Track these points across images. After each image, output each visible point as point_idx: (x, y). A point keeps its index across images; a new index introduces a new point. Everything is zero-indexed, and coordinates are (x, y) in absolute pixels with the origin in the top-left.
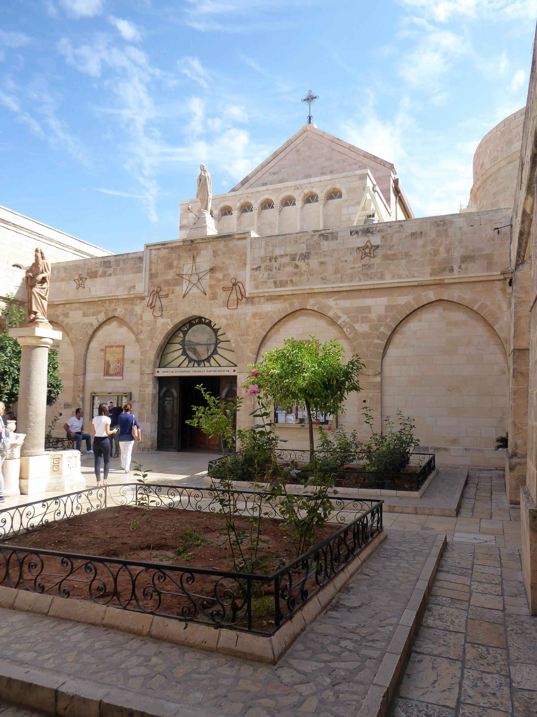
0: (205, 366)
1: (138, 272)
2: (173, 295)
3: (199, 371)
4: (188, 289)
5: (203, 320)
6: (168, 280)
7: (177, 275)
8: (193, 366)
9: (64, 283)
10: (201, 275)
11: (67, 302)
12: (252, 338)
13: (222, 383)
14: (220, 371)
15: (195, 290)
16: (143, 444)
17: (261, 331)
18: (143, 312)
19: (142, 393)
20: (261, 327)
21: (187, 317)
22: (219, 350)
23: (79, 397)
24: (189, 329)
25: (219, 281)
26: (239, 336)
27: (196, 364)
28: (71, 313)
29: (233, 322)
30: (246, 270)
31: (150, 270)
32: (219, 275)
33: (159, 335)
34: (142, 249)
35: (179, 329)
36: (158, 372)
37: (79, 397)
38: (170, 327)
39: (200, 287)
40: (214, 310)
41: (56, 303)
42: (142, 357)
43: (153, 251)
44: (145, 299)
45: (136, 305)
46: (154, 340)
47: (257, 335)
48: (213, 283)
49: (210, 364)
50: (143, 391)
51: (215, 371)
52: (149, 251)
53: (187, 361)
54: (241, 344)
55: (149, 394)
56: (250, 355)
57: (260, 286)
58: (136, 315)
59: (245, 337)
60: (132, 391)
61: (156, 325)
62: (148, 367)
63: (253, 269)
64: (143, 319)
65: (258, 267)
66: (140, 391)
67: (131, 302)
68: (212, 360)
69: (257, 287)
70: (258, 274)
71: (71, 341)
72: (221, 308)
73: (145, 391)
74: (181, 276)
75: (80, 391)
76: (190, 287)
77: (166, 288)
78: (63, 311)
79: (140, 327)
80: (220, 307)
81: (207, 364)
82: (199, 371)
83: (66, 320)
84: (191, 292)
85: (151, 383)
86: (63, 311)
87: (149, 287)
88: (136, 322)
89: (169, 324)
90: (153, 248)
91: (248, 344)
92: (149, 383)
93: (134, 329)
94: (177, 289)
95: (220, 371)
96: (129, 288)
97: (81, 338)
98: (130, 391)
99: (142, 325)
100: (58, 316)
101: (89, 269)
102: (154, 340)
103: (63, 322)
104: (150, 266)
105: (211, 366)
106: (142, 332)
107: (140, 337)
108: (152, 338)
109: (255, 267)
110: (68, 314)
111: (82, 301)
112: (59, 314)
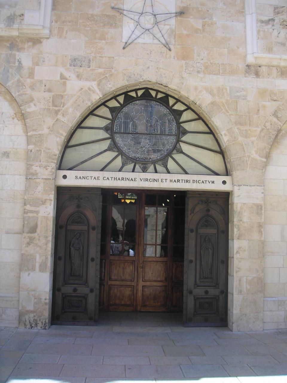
0: (156, 172)
2: (104, 42)
3: (154, 180)
4: (134, 37)
5: (153, 93)
6: (93, 15)
7: (113, 8)
8: (133, 171)
10: (159, 18)
12: (259, 129)
13: (190, 204)
14: (198, 182)
15: (147, 39)
16: (32, 315)
17: (275, 120)
18: (37, 65)
19: (30, 215)
20: (275, 114)
21: (133, 82)
22: (185, 147)
24: (123, 106)
25: (197, 31)
26: (236, 123)
27: (137, 166)
29: (224, 101)
30: (245, 22)
32: (195, 22)
33: (71, 110)
35: (104, 104)
36: (65, 177)
38: (97, 97)
39: (159, 35)
40: (185, 75)
44: (41, 42)
45: (19, 50)
47: (268, 125)
48: (185, 32)
49: (167, 169)
50: (31, 212)
51: (187, 181)
53: (119, 161)
54: (240, 139)
55: (47, 218)
56: (257, 157)
57: (275, 49)
58: (20, 67)
59: (247, 128)
61: (64, 91)
62: (46, 167)
63: (262, 22)
64: (37, 77)
65: (270, 20)
66: (25, 212)
68: (171, 164)
69: (269, 50)
70: (271, 30)
72: (199, 75)
73: (37, 212)
74: (120, 11)
76: (137, 33)
77: (89, 29)
79: (29, 91)
80: (198, 72)
81: (159, 168)
82: (154, 180)
84: (140, 40)
88: (19, 81)
89: (94, 92)
91: (254, 139)
92: (45, 197)
93: (15, 94)
94: (112, 31)
95: (198, 182)
99: (32, 88)
102: (60, 116)
105: (169, 172)
106: (32, 100)
107: (29, 110)
108: (57, 112)
109: (265, 18)
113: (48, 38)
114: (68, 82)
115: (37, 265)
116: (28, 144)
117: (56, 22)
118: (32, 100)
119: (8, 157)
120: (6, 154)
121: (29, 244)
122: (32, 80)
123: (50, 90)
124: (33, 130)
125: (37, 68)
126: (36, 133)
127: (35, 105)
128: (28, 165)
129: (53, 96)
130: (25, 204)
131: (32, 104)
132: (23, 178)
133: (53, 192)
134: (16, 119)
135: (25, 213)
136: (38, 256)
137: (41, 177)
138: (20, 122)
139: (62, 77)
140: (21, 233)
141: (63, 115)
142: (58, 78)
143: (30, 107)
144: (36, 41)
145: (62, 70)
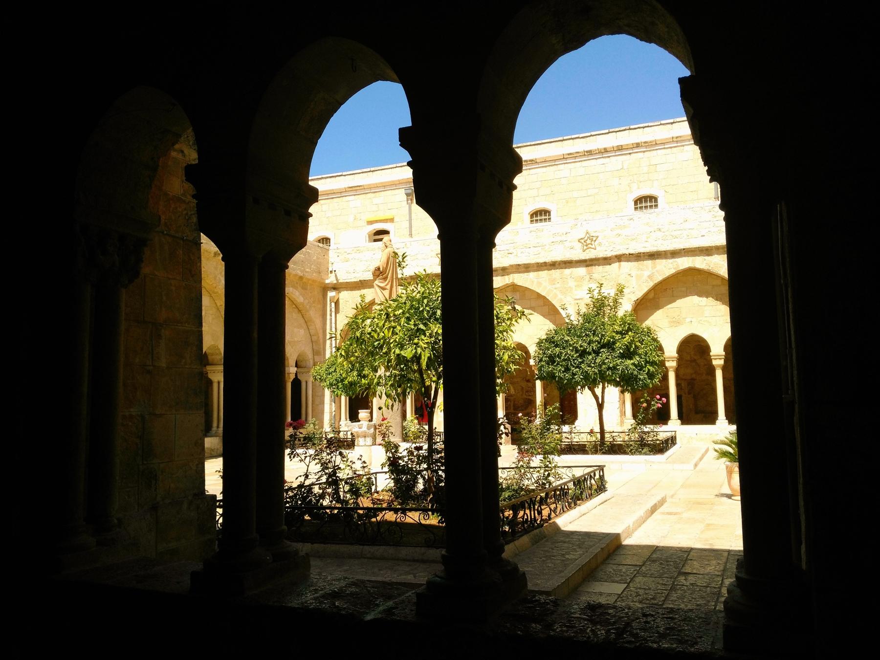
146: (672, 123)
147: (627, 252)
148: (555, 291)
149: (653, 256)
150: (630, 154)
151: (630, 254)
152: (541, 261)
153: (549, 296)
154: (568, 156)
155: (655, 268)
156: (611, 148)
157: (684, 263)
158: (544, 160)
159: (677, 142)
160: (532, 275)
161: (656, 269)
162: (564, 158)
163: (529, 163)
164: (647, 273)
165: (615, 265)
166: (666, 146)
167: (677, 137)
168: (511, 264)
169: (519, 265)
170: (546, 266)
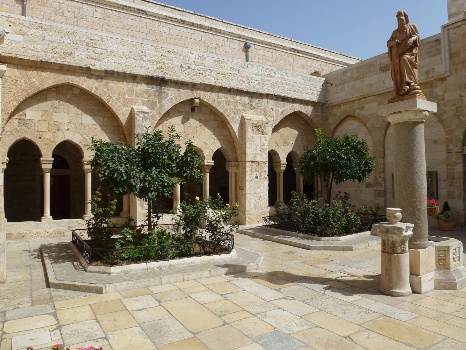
1: (435, 55)
9: (357, 82)
11: (362, 97)
18: (445, 92)
23: (380, 177)
28: (367, 106)
31: (450, 50)
34: (438, 31)
37: (380, 177)
41: (351, 100)
42: (447, 136)
43: (451, 32)
45: (435, 87)
46: (461, 118)
50: (451, 169)
52: (446, 32)
60: (437, 170)
62: (456, 146)
66: (448, 169)
67: (429, 86)
71: (369, 130)
73: (454, 169)
75: (381, 172)
78: (359, 105)
83: (362, 113)
85: (461, 161)
86: (359, 105)
87: (450, 67)
90: (452, 27)
96: (427, 72)
97: (378, 126)
98: (435, 170)
100: (354, 111)
101: (381, 64)
102: (461, 118)
103: (359, 114)
104: (449, 46)
106: (445, 112)
107: (444, 117)
110: (364, 107)
111: (376, 94)
112: (355, 108)
113: (449, 76)
114: (464, 98)
115: (456, 196)
116: (446, 135)
117: (453, 66)
118: (445, 112)
119: (437, 143)
120: (436, 142)
121: (451, 186)
122: (444, 102)
123: (454, 105)
124: (448, 128)
125: (446, 94)
126: (449, 129)
127: (447, 114)
128: (447, 146)
129: (456, 108)
130: (447, 166)
131: (445, 114)
132: (446, 152)
133: (462, 158)
134: (439, 124)
135: (448, 170)
136: (456, 192)
137: (454, 151)
138: (441, 124)
139: (461, 96)
140: (447, 180)
141: (463, 117)
142: (458, 97)
143: (444, 116)
144: (443, 79)
145: (460, 92)
146: (228, 24)
147: (274, 93)
148: (229, 110)
149: (285, 99)
150: (206, 32)
151: (275, 95)
152: (223, 85)
153: (225, 113)
154: (169, 19)
155: (285, 107)
156: (196, 24)
157: (298, 107)
158: (152, 15)
159: (231, 36)
160: (214, 95)
161: (285, 108)
162: (166, 19)
163: (140, 12)
164: (281, 110)
165: (265, 100)
166: (225, 36)
167: (232, 33)
168: (202, 82)
169: (207, 85)
170: (225, 90)
